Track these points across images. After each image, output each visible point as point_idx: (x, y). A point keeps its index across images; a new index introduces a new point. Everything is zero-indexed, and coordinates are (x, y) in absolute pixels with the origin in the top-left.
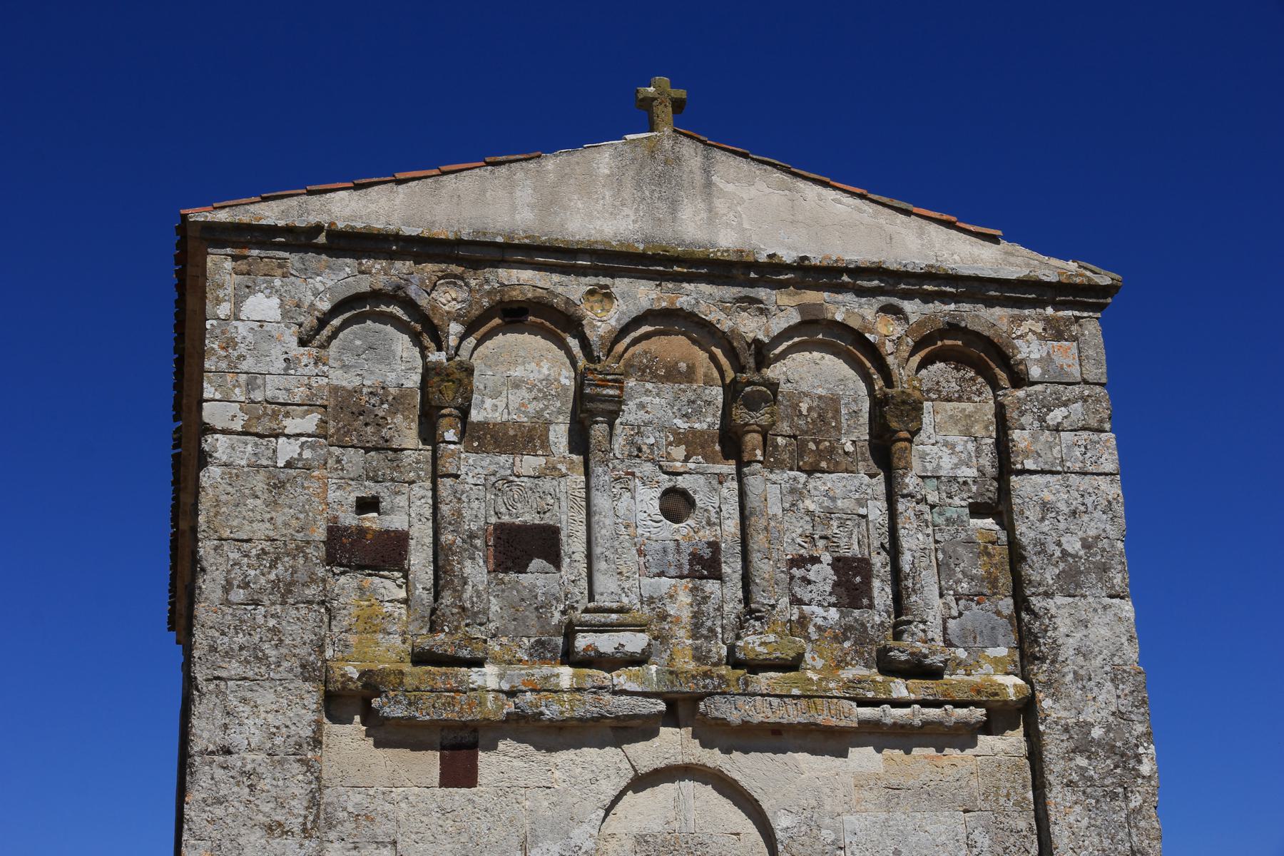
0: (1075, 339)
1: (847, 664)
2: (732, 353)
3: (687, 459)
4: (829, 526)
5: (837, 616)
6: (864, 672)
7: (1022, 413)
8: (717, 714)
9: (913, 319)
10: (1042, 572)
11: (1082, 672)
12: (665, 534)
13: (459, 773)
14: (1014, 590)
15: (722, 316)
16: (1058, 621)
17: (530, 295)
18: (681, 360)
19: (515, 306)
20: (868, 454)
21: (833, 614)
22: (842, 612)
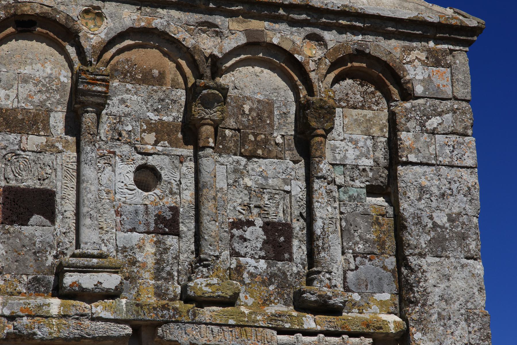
0: (449, 66)
1: (271, 302)
2: (194, 64)
3: (156, 143)
4: (262, 198)
5: (265, 266)
6: (284, 309)
7: (408, 120)
8: (171, 337)
9: (331, 45)
10: (418, 238)
11: (444, 313)
12: (138, 200)
14: (397, 251)
15: (187, 35)
16: (428, 275)
17: (38, 11)
18: (155, 68)
19: (26, 19)
20: (293, 146)
21: (262, 264)
22: (269, 263)
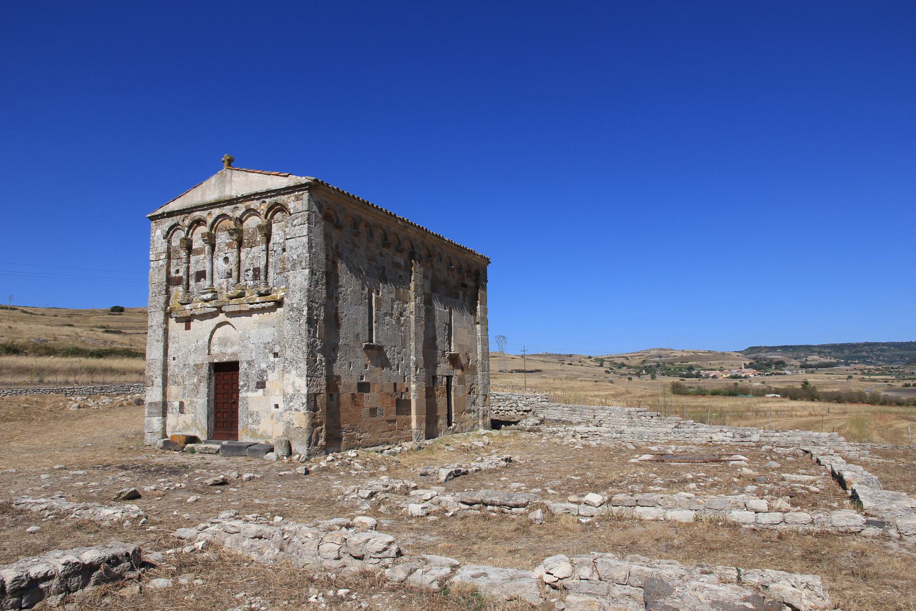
13: (188, 328)
